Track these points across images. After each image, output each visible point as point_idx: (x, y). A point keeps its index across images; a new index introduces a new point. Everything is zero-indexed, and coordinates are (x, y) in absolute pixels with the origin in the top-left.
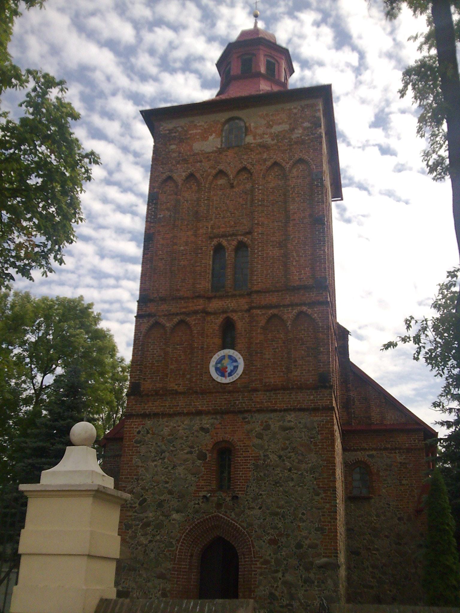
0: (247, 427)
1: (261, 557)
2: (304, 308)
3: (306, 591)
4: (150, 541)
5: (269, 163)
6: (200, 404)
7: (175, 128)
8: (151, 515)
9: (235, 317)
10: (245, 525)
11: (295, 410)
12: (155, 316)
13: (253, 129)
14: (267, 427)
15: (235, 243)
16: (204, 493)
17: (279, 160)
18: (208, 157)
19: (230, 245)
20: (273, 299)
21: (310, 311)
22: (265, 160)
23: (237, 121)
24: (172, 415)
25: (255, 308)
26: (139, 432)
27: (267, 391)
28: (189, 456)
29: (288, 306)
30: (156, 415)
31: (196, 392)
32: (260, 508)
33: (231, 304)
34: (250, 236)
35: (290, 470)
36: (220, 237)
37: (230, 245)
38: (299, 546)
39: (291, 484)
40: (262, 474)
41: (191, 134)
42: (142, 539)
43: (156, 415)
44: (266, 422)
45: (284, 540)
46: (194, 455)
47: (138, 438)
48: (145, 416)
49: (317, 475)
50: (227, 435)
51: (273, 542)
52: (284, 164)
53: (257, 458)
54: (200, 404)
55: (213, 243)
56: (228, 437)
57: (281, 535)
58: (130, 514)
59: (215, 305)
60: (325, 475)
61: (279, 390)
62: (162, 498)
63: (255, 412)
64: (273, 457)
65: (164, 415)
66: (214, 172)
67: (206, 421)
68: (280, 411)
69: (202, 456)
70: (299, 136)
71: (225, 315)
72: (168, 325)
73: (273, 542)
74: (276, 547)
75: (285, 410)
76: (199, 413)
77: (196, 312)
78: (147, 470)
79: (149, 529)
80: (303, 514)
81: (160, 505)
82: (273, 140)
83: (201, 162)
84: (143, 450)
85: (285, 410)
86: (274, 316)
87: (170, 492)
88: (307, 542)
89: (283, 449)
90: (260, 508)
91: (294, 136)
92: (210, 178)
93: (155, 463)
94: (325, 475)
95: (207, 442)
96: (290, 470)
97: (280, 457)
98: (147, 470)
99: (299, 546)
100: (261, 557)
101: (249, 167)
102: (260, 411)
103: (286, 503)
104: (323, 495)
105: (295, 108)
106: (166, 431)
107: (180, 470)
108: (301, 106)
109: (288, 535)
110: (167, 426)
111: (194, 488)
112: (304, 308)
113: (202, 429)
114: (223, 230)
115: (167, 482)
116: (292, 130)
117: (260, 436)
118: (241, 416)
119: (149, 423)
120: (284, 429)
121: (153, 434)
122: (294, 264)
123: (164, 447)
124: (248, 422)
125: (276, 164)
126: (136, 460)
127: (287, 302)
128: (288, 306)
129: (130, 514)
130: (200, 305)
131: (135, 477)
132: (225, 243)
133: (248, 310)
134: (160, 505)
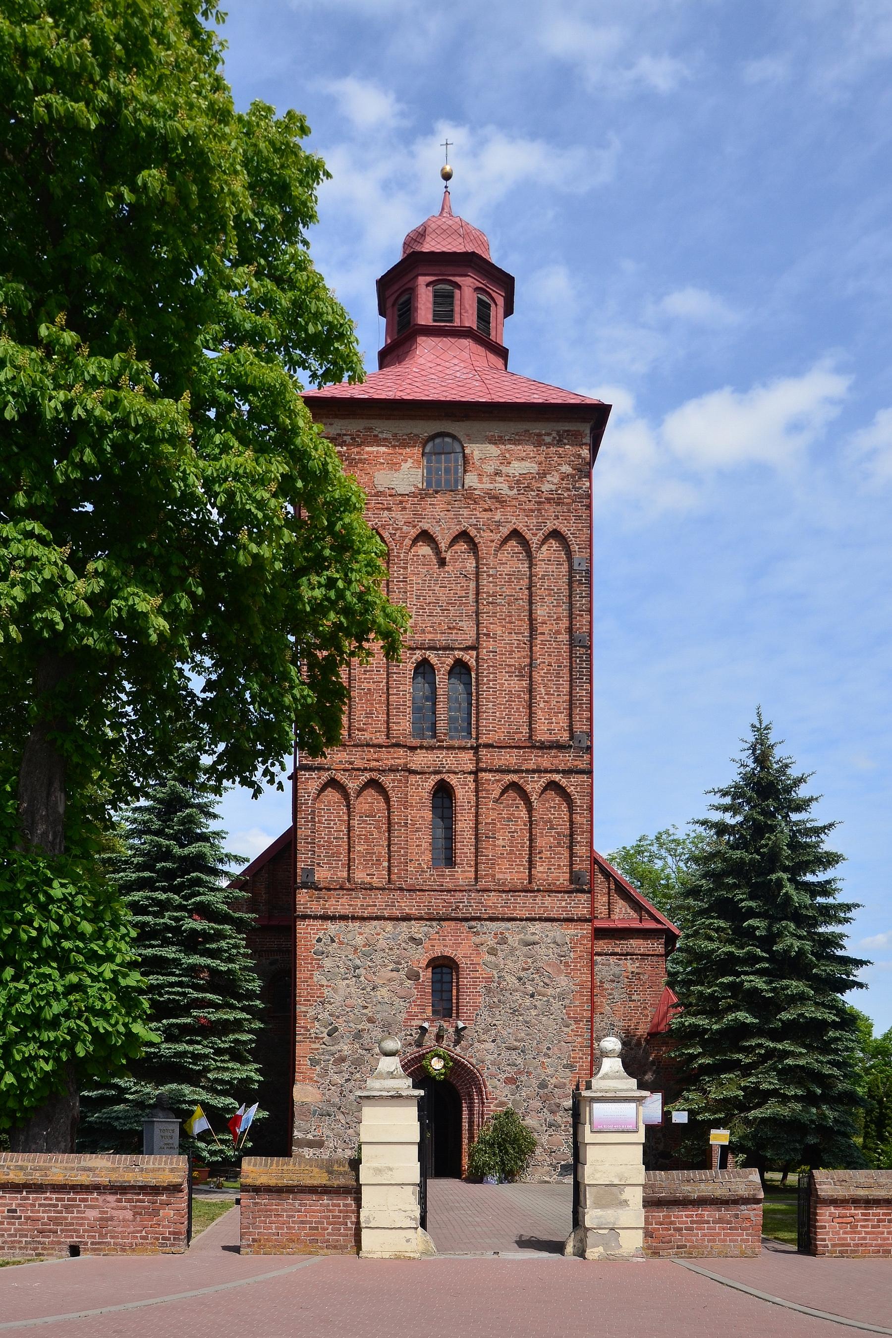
0: (477, 939)
1: (496, 1099)
2: (557, 777)
3: (550, 1136)
4: (348, 1080)
5: (505, 531)
6: (407, 905)
7: (339, 435)
8: (346, 1047)
9: (453, 780)
10: (474, 1061)
11: (540, 919)
12: (329, 769)
13: (478, 463)
14: (504, 941)
15: (450, 661)
16: (419, 1023)
17: (521, 527)
18: (401, 502)
19: (442, 663)
20: (509, 758)
21: (564, 782)
22: (499, 524)
23: (448, 440)
24: (363, 919)
25: (485, 770)
26: (319, 940)
27: (504, 891)
28: (395, 974)
29: (534, 771)
30: (344, 918)
31: (401, 889)
32: (493, 1041)
33: (448, 759)
34: (475, 652)
35: (532, 996)
36: (425, 649)
37: (442, 663)
38: (543, 1085)
39: (534, 1012)
40: (496, 1000)
41: (367, 453)
42: (335, 1076)
43: (344, 918)
44: (502, 933)
45: (524, 1078)
46: (402, 974)
47: (319, 947)
48: (325, 918)
49: (567, 1002)
50: (447, 949)
51: (510, 1081)
52: (528, 536)
53: (490, 979)
54: (407, 905)
55: (415, 657)
56: (448, 952)
57: (520, 1073)
58: (314, 1046)
59: (420, 760)
60: (577, 1003)
61: (519, 891)
62: (360, 1027)
63: (485, 920)
64: (511, 980)
65: (354, 918)
66: (414, 532)
67: (418, 929)
68: (521, 920)
69: (413, 976)
70: (554, 487)
71: (438, 777)
72: (350, 785)
73: (510, 1081)
74: (514, 1087)
75: (527, 919)
76: (407, 918)
77: (393, 770)
78: (335, 991)
79: (345, 1066)
80: (548, 1048)
81: (358, 1035)
82: (511, 488)
83: (389, 509)
84: (327, 963)
85: (527, 919)
86: (514, 786)
87: (371, 1020)
88: (553, 1081)
89: (524, 969)
90: (493, 1041)
91: (546, 487)
92: (408, 542)
93: (347, 982)
94: (577, 1003)
95: (420, 957)
96: (532, 996)
97: (520, 979)
98: (335, 991)
99: (543, 1085)
100: (496, 1099)
101: (473, 532)
102: (492, 919)
103: (527, 1035)
104: (574, 1027)
105: (549, 434)
106: (360, 940)
107: (383, 992)
108: (558, 432)
109: (529, 1073)
110: (360, 934)
111: (405, 1015)
112: (557, 777)
113: (412, 939)
114: (430, 636)
115: (366, 1007)
116: (542, 475)
117: (493, 952)
118: (466, 924)
119: (333, 928)
120: (527, 944)
121: (341, 943)
122: (542, 705)
123: (358, 962)
124: (477, 933)
125: (515, 534)
126: (317, 977)
127: (531, 766)
128: (534, 771)
129: (314, 1046)
130: (400, 757)
131: (318, 1000)
132: (434, 660)
133: (475, 773)
134: (358, 1035)
